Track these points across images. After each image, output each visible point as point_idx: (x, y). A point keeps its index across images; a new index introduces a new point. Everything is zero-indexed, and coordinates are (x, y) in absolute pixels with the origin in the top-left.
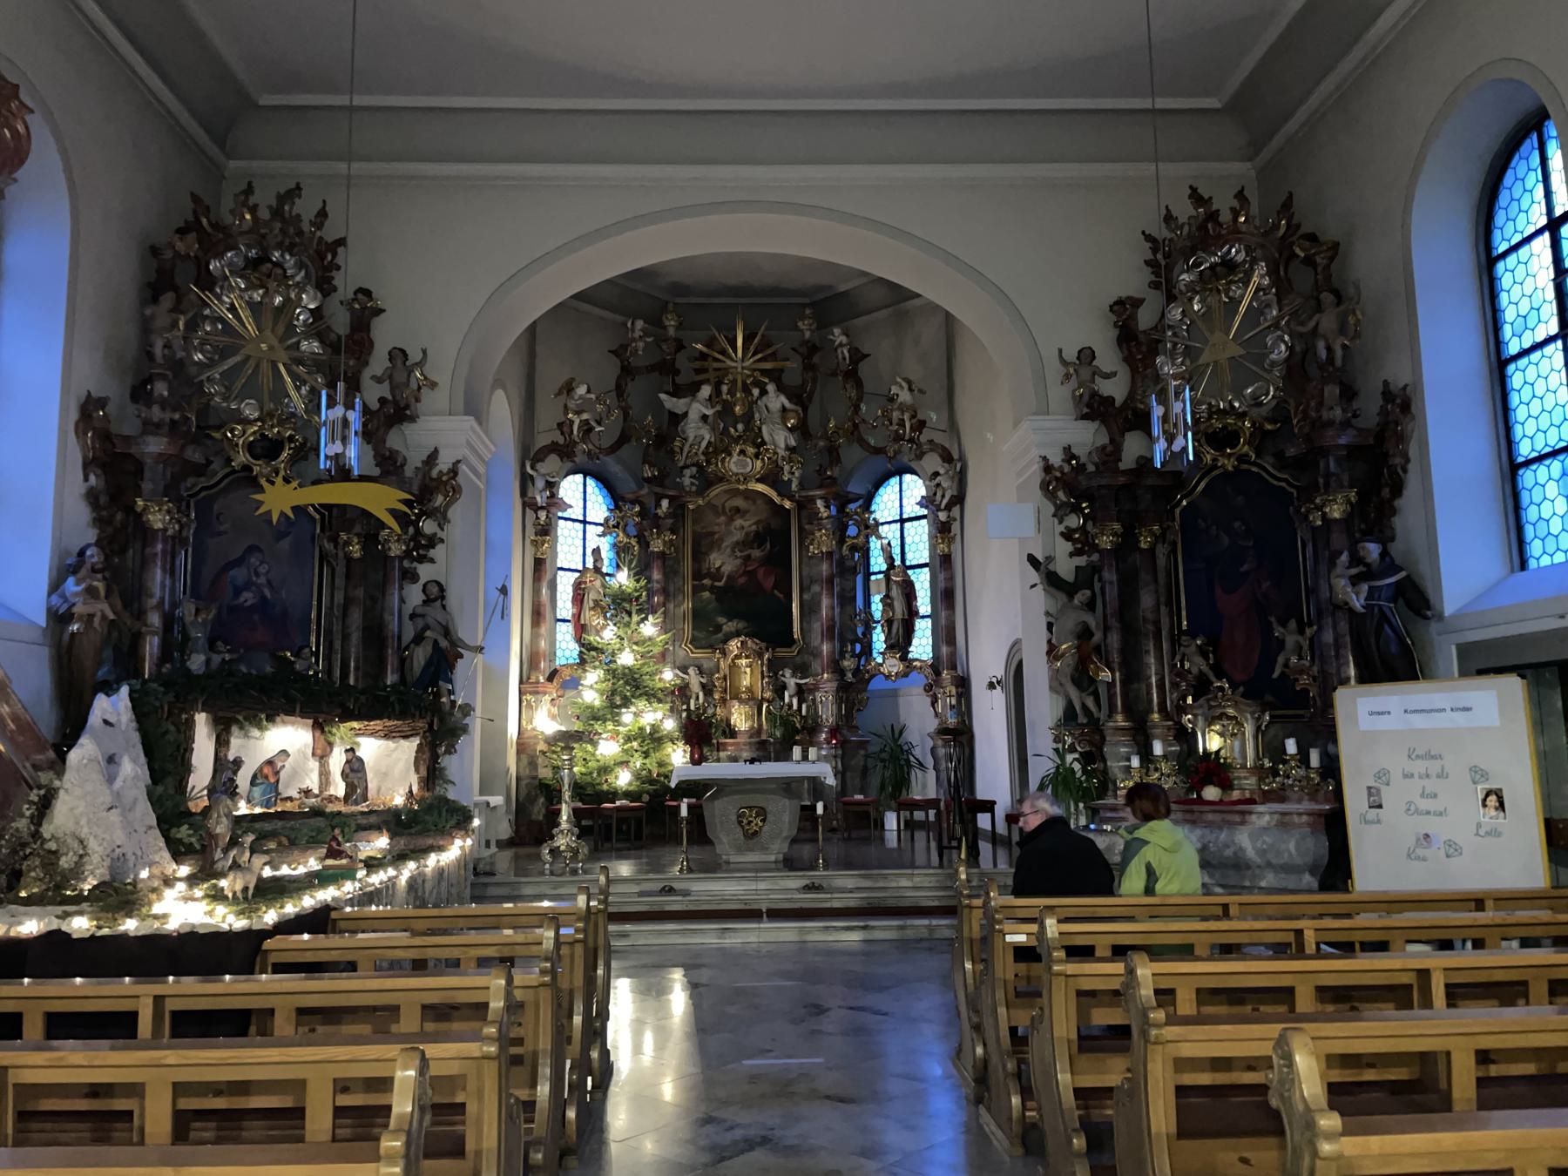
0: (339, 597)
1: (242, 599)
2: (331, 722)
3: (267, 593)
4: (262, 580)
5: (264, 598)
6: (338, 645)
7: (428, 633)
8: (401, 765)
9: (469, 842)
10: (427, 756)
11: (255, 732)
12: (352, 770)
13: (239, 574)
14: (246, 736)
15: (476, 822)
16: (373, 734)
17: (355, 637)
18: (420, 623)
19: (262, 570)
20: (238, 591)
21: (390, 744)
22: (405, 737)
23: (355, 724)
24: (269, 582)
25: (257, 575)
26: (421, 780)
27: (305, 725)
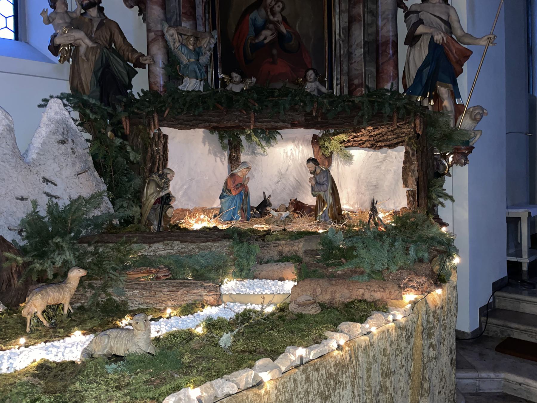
0: (345, 18)
1: (262, 38)
2: (327, 136)
3: (283, 29)
4: (278, 18)
5: (280, 34)
6: (345, 68)
7: (420, 29)
8: (390, 177)
9: (438, 294)
10: (415, 166)
11: (260, 150)
12: (318, 183)
13: (258, 16)
14: (254, 153)
15: (456, 260)
16: (361, 145)
17: (359, 52)
18: (413, 18)
19: (277, 9)
20: (258, 32)
21: (378, 155)
22: (392, 146)
23: (343, 137)
24: (284, 19)
25: (274, 14)
26: (410, 194)
27: (304, 141)
